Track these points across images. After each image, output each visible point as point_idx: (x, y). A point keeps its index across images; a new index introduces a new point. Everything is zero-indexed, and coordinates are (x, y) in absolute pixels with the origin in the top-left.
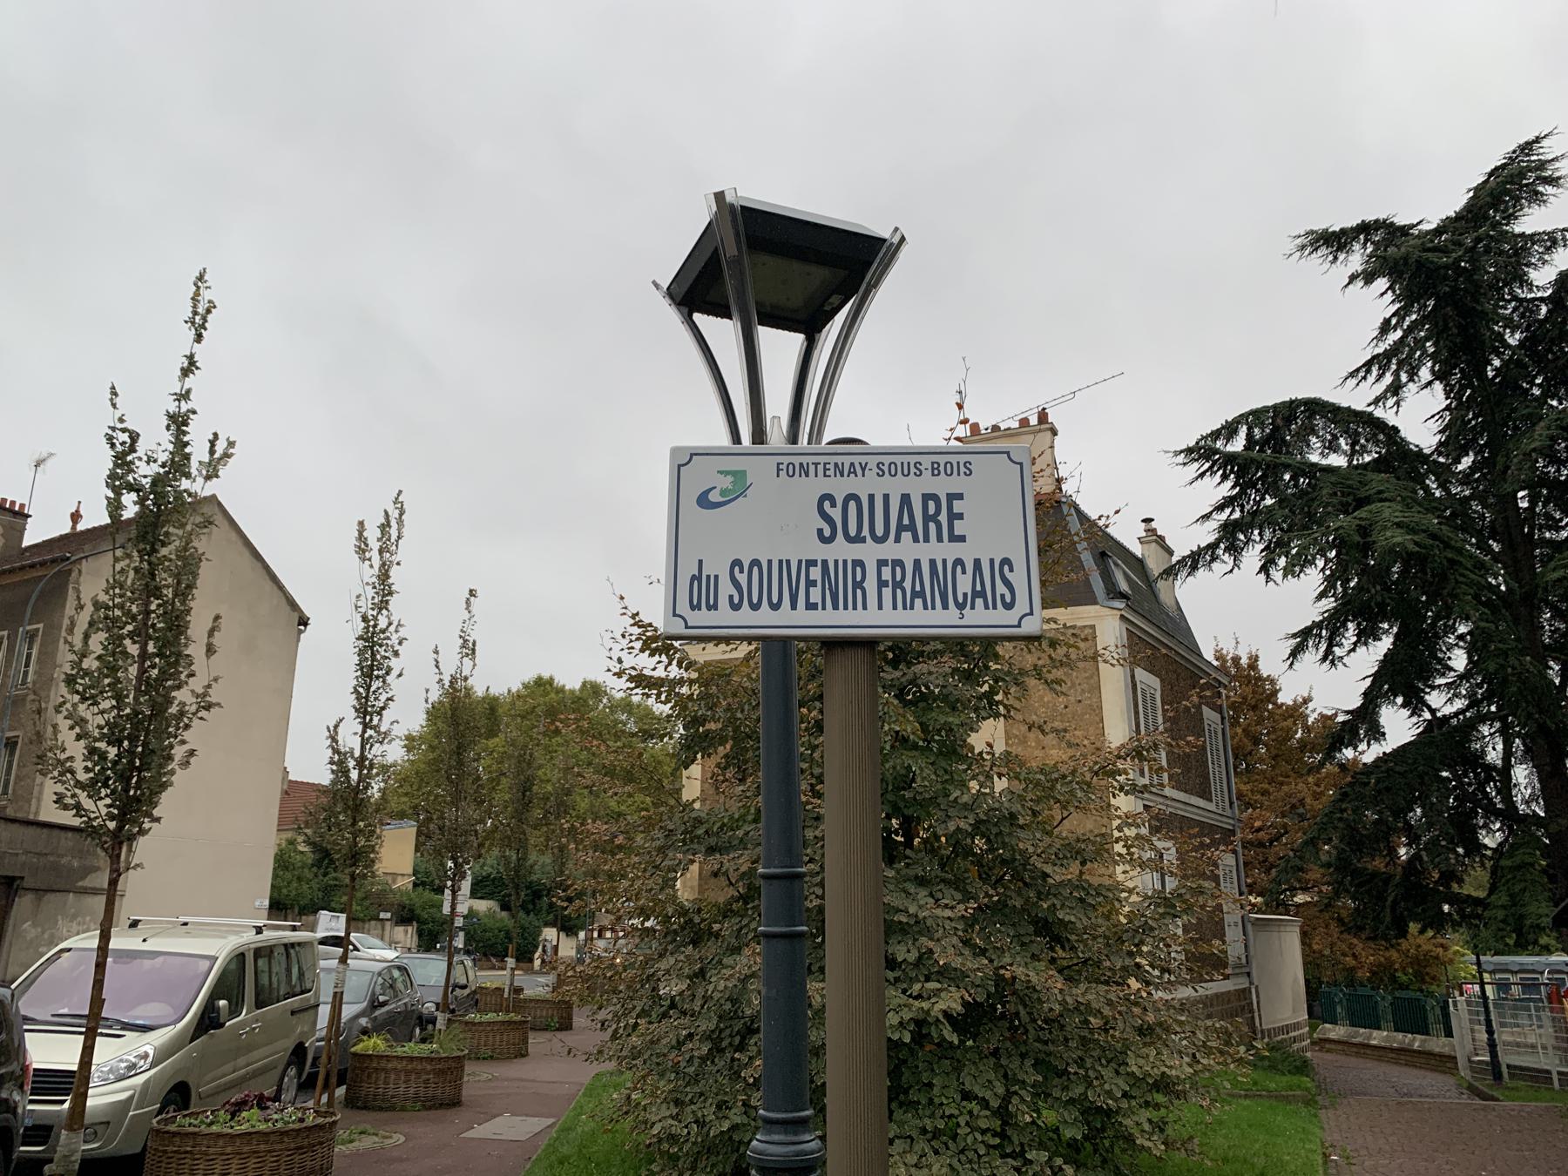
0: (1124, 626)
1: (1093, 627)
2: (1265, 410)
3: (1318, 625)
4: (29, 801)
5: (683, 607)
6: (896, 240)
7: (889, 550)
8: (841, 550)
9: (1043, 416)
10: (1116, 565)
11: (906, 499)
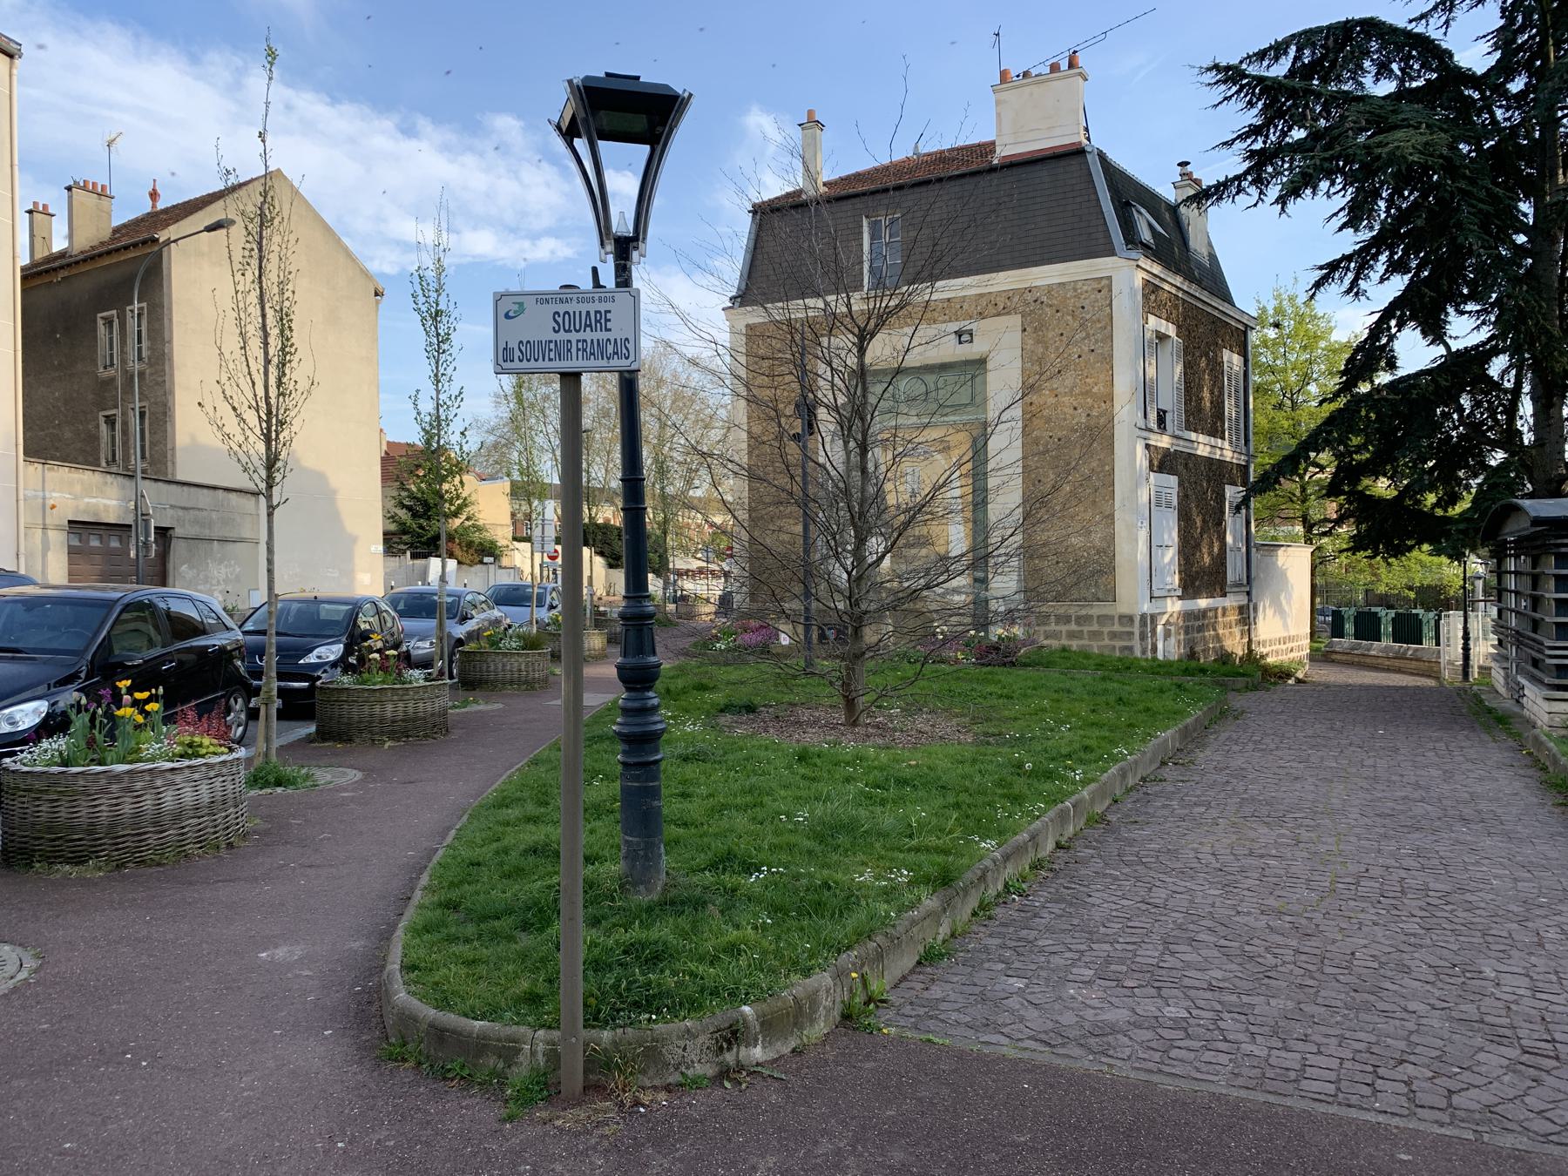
1: (1110, 278)
2: (1319, 30)
3: (1347, 258)
4: (165, 464)
5: (501, 361)
6: (686, 95)
7: (581, 335)
8: (562, 336)
11: (588, 313)
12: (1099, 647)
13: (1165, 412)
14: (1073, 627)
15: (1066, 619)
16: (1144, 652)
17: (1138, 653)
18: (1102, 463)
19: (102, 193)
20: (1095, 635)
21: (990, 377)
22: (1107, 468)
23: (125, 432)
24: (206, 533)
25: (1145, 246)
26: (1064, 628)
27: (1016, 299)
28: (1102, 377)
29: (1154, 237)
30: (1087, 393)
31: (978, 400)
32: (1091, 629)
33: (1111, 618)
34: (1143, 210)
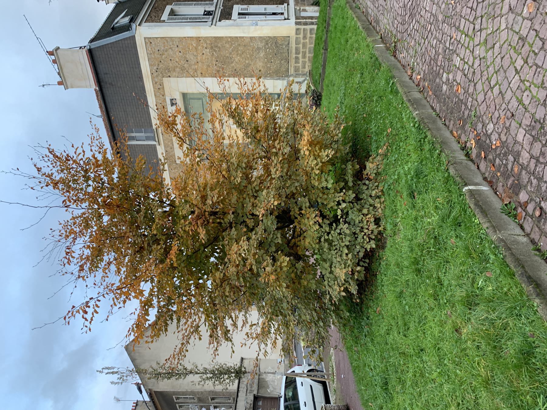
0: (144, 24)
1: (145, 38)
9: (51, 53)
10: (117, 23)
12: (311, 43)
13: (205, 11)
14: (300, 56)
15: (297, 58)
16: (312, 23)
17: (315, 27)
18: (227, 42)
19: (137, 404)
20: (304, 45)
21: (190, 91)
22: (229, 40)
23: (220, 403)
24: (256, 381)
25: (132, 20)
26: (301, 60)
27: (156, 80)
28: (189, 42)
29: (128, 16)
30: (196, 49)
31: (200, 97)
32: (301, 48)
33: (297, 38)
34: (116, 21)
